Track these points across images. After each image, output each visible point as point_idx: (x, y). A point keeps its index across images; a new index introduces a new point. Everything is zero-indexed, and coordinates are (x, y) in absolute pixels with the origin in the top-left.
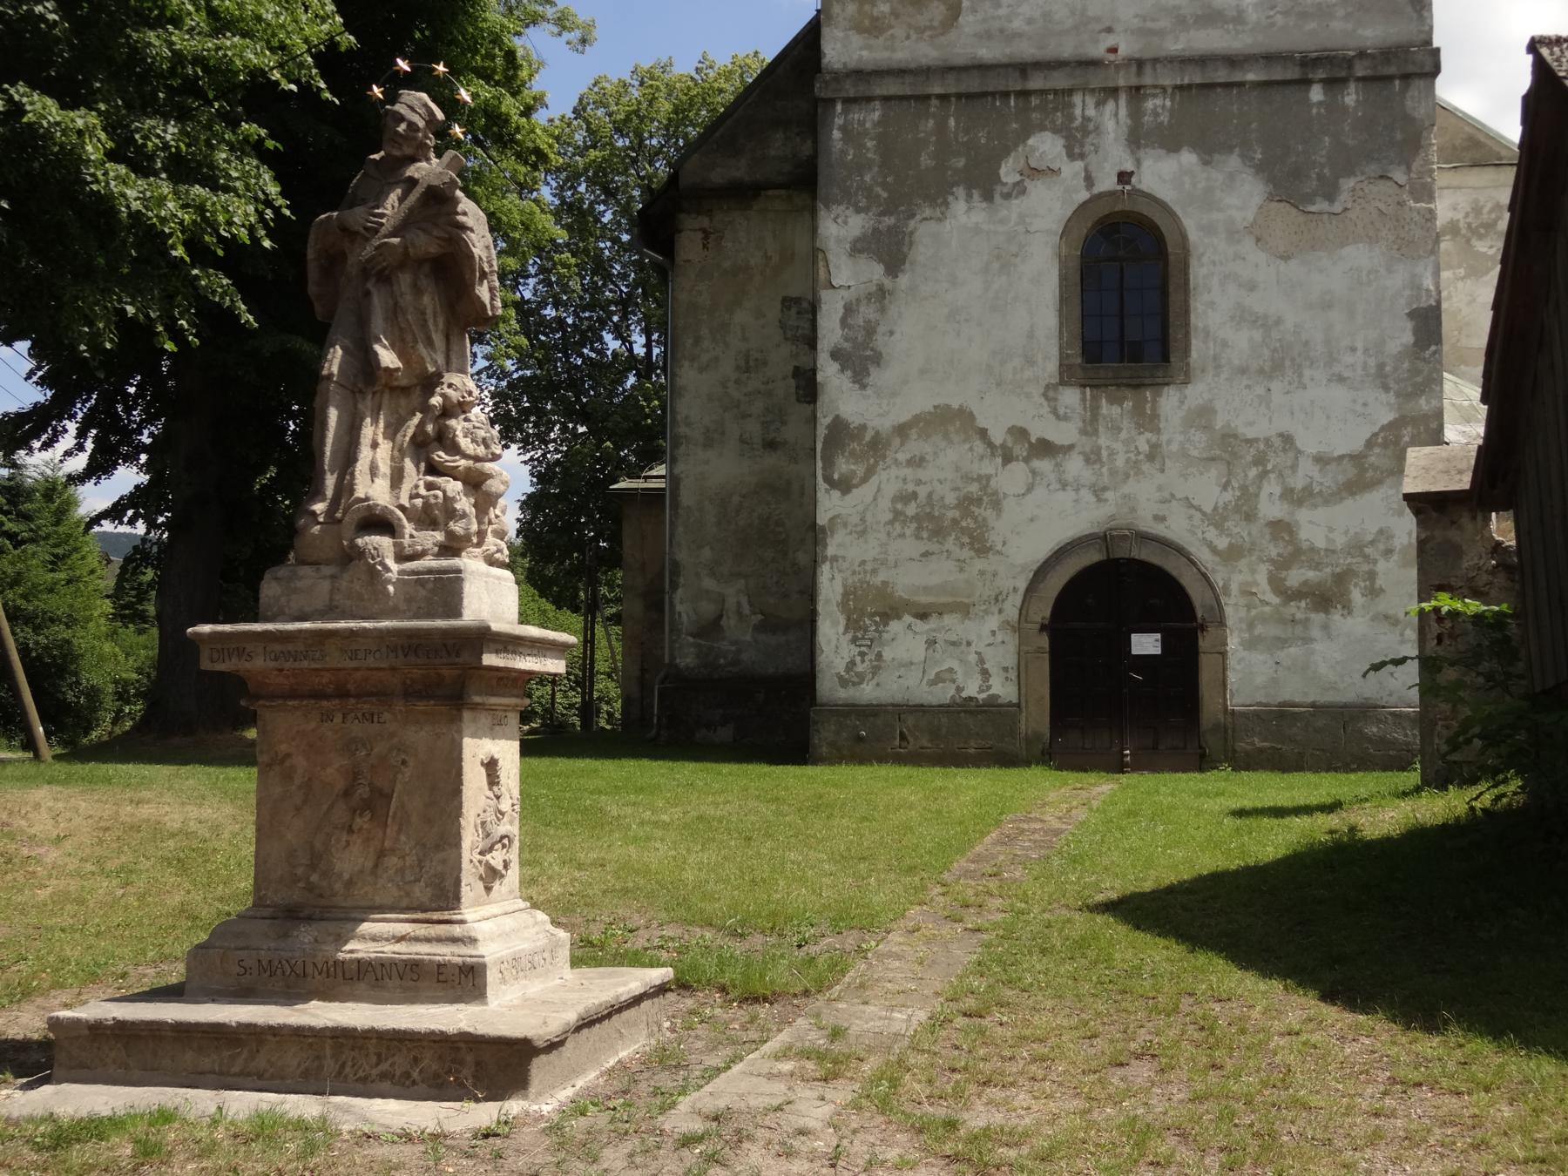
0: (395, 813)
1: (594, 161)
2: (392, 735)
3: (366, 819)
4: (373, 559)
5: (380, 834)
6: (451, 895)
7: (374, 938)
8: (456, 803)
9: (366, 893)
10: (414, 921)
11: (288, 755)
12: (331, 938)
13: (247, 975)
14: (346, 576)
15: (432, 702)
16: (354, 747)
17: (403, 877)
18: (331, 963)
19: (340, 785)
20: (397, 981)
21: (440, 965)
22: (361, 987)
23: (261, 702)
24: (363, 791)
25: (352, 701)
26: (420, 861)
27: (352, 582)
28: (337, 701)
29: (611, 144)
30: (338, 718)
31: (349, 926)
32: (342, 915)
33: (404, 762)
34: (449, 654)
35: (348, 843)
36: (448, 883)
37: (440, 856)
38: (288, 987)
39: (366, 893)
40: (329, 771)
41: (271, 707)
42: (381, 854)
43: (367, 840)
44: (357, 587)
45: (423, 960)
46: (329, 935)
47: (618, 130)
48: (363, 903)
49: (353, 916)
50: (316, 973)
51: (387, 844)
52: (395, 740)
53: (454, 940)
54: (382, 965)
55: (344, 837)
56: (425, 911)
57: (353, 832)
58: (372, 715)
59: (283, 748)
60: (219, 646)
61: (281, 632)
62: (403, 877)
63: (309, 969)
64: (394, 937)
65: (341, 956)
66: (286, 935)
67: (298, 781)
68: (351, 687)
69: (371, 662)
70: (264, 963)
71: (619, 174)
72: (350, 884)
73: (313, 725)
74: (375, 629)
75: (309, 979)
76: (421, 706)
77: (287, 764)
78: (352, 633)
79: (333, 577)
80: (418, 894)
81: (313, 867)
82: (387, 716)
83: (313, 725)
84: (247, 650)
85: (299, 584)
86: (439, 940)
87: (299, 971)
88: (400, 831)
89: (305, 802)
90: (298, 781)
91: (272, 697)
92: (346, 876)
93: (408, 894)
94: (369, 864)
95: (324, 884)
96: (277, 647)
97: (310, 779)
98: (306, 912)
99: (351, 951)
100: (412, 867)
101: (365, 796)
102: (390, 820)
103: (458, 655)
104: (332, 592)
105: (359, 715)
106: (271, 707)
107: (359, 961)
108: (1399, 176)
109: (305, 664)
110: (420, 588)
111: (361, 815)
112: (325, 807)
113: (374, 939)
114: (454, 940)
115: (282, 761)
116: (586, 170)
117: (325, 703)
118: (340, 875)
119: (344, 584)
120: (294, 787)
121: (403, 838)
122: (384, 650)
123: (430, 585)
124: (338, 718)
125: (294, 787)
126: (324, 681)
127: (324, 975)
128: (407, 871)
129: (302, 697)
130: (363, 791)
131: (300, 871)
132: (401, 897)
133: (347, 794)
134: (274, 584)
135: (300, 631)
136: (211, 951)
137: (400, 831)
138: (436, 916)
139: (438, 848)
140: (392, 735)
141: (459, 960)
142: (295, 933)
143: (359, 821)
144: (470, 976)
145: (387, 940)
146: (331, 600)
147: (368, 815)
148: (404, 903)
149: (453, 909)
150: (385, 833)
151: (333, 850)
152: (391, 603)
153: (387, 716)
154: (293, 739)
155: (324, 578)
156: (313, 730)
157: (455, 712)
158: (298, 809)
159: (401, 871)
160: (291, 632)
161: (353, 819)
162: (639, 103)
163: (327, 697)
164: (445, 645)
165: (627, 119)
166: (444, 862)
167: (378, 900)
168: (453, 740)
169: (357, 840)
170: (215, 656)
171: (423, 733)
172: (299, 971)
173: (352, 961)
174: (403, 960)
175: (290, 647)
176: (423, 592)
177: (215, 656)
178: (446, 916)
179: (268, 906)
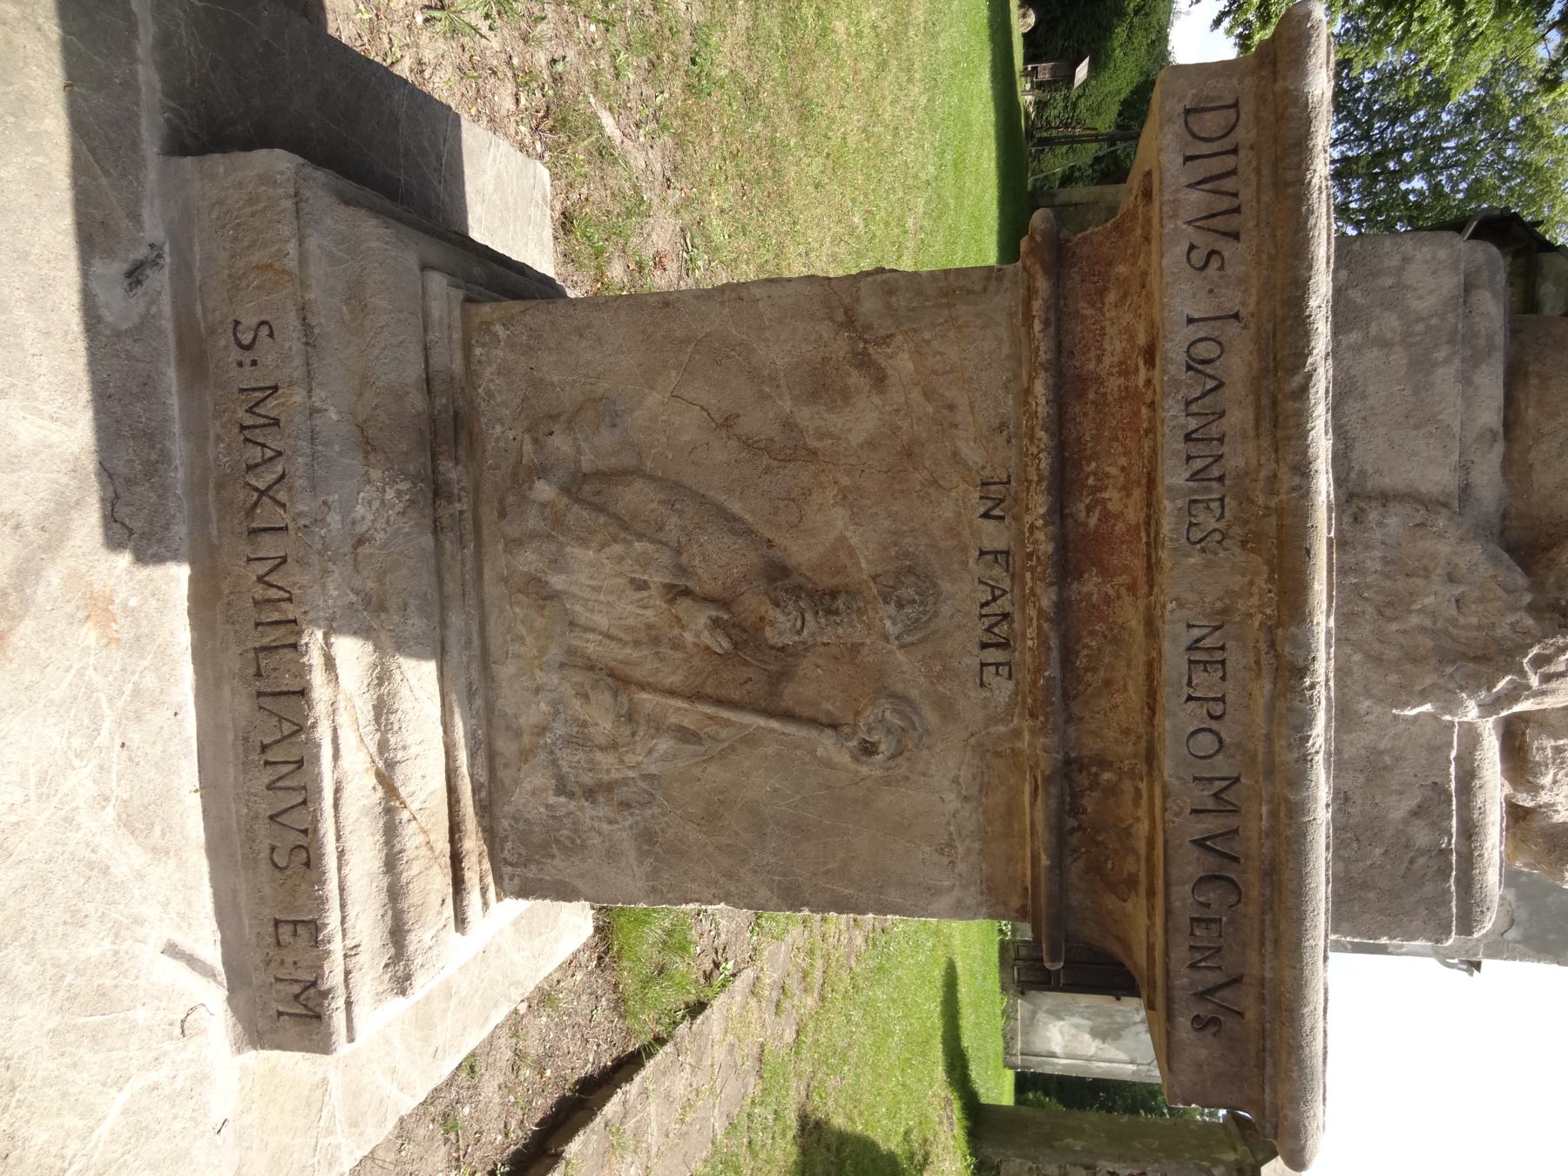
0: (727, 723)
1: (1500, 103)
2: (946, 709)
3: (706, 638)
4: (1539, 662)
5: (674, 680)
6: (532, 872)
7: (382, 710)
8: (763, 893)
9: (521, 639)
10: (452, 790)
11: (880, 381)
12: (370, 584)
13: (235, 354)
14: (1475, 558)
15: (1045, 861)
16: (908, 593)
17: (569, 741)
18: (291, 611)
19: (801, 553)
20: (265, 809)
21: (315, 927)
22: (239, 703)
23: (1042, 284)
24: (781, 627)
25: (1047, 599)
26: (610, 787)
27: (1451, 579)
28: (1046, 547)
29: (1514, 115)
30: (995, 536)
31: (416, 624)
32: (452, 587)
33: (868, 749)
34: (1203, 995)
35: (641, 586)
36: (559, 866)
37: (627, 845)
38: (220, 486)
39: (521, 639)
40: (839, 516)
41: (1028, 317)
42: (619, 680)
43: (653, 638)
44: (1434, 597)
45: (321, 881)
46: (380, 580)
47: (1524, 120)
48: (494, 628)
49: (456, 620)
50: (262, 568)
51: (648, 701)
52: (932, 718)
53: (397, 934)
54: (300, 763)
55: (657, 579)
56: (485, 809)
57: (672, 601)
58: (1004, 645)
59: (902, 363)
60: (1245, 134)
61: (1304, 389)
62: (569, 741)
63: (270, 546)
64: (391, 765)
65: (314, 639)
66: (368, 446)
67: (807, 416)
68: (1091, 585)
69: (1178, 719)
70: (270, 408)
71: (1483, 125)
72: (545, 596)
73: (972, 454)
74: (1305, 759)
75: (248, 550)
76: (1035, 813)
77: (856, 378)
78: (1292, 672)
79: (1466, 489)
80: (527, 786)
81: (577, 485)
82: (1003, 689)
83: (972, 454)
84: (1228, 248)
85: (1445, 377)
86: (395, 894)
87: (267, 515)
88: (685, 735)
89: (747, 443)
90: (807, 416)
91: (1060, 317)
92: (557, 581)
93: (525, 755)
94: (592, 646)
95: (533, 521)
96: (1238, 365)
97: (814, 453)
98: (453, 473)
99: (330, 664)
100: (593, 767)
101: (768, 632)
102: (710, 710)
103: (1200, 1024)
104: (1411, 497)
105: (1004, 604)
106: (1028, 317)
107: (303, 693)
108: (1512, 934)
109: (1174, 476)
110: (1408, 804)
111: (716, 623)
112: (736, 507)
113: (382, 710)
114: (397, 934)
115: (863, 361)
116: (1494, 97)
117: (1040, 504)
118: (557, 564)
119: (1444, 549)
120: (787, 405)
121: (664, 744)
122: (1223, 766)
123: (1422, 836)
124: (995, 536)
125: (787, 405)
126: (1112, 495)
127: (260, 592)
128: (580, 755)
129: (1060, 420)
130: (781, 627)
131: (560, 443)
132: (518, 734)
133: (777, 574)
134: (1450, 283)
135: (1303, 470)
136: (286, 230)
137: (685, 735)
138: (472, 843)
139: (647, 837)
140: (946, 709)
141: (334, 975)
142: (375, 474)
143: (700, 618)
144: (300, 1010)
145: (383, 746)
146: (1385, 498)
147: (722, 644)
148: (505, 746)
149: (498, 880)
150: (672, 693)
151: (618, 548)
152: (1364, 705)
153: (1003, 689)
154: (928, 395)
155: (1464, 468)
156: (955, 454)
157: (1016, 902)
158: (727, 423)
159: (580, 739)
160: (1302, 432)
161: (707, 599)
162: (1550, 137)
163: (1060, 512)
164: (1236, 981)
165: (1534, 127)
166: (612, 854)
167: (506, 671)
168: (934, 892)
169: (654, 610)
170: (1211, 123)
171: (952, 801)
172: (267, 515)
173: (303, 671)
174: (316, 821)
175: (1239, 417)
176: (1399, 809)
177: (1211, 123)
178: (476, 867)
179: (467, 349)
